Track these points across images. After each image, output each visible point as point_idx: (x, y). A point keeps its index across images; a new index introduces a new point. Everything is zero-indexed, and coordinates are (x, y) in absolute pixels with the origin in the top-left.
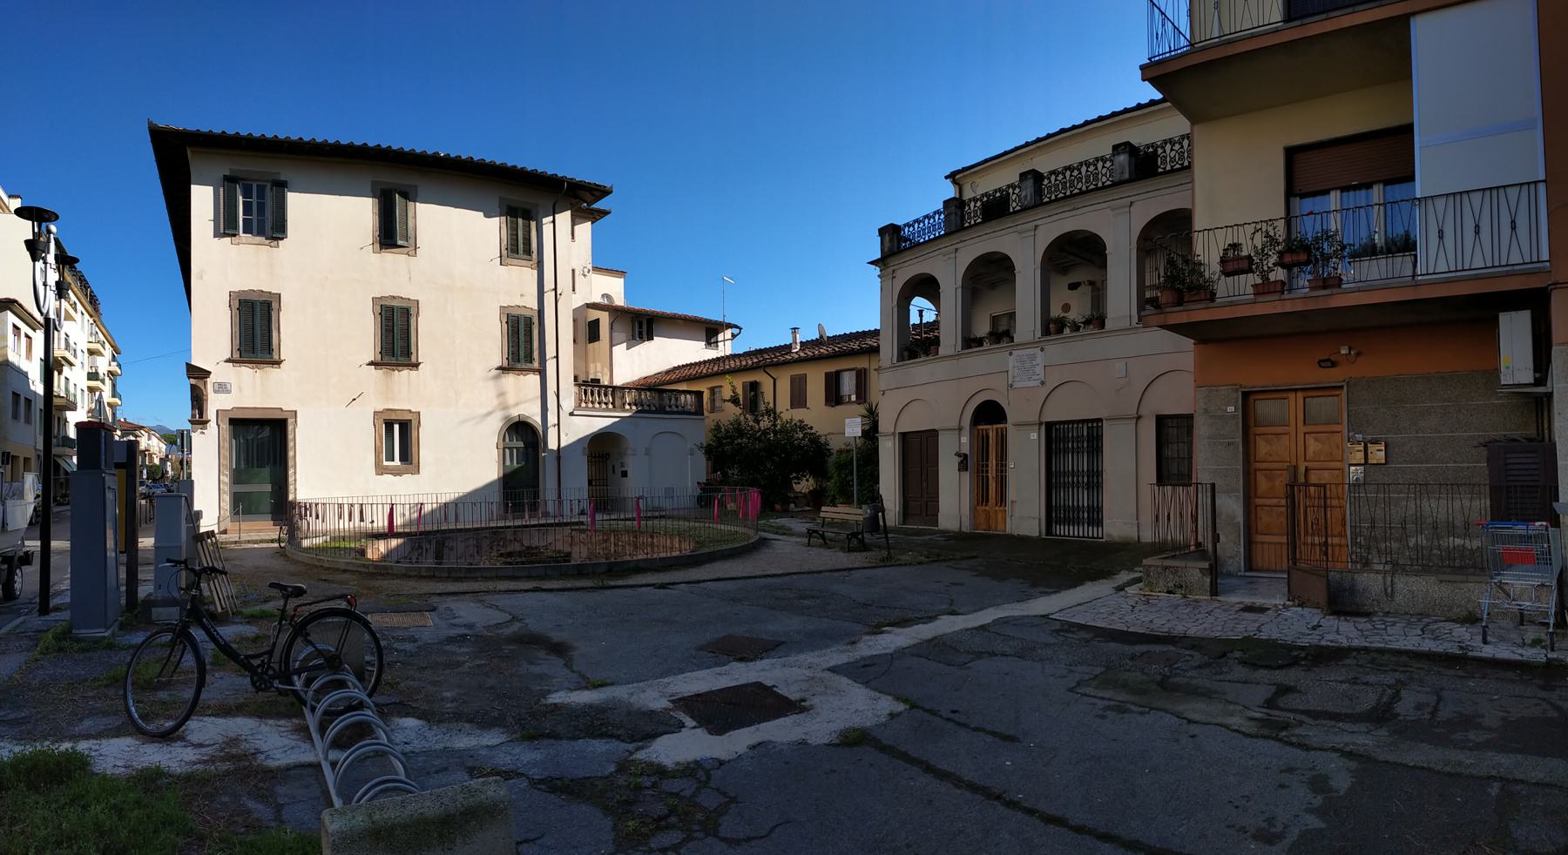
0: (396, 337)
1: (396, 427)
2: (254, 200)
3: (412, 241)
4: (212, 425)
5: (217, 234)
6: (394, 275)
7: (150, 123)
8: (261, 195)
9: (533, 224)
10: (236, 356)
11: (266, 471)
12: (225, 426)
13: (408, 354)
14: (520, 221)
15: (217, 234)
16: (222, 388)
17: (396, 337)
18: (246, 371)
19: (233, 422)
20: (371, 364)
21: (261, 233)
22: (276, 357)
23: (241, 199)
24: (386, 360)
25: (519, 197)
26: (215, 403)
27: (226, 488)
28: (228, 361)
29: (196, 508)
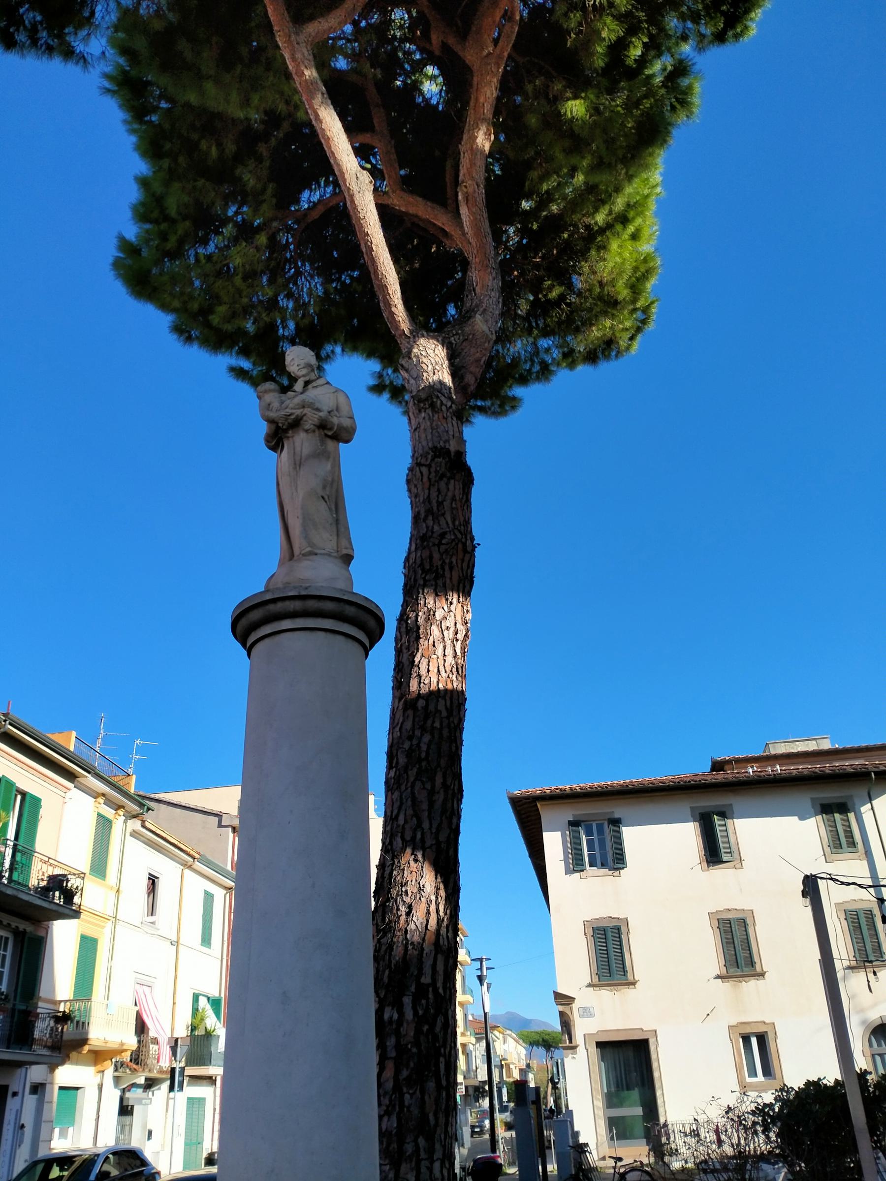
0: (738, 948)
1: (754, 1041)
2: (595, 837)
3: (736, 855)
4: (581, 1050)
5: (568, 872)
6: (725, 889)
7: (508, 793)
8: (601, 831)
9: (851, 816)
10: (596, 980)
11: (635, 1094)
12: (593, 1049)
13: (752, 964)
14: (837, 816)
15: (568, 872)
16: (586, 1012)
17: (738, 948)
18: (605, 994)
19: (599, 1045)
20: (718, 977)
21: (603, 865)
22: (630, 978)
23: (584, 838)
24: (733, 971)
25: (831, 794)
26: (582, 1028)
27: (600, 1113)
28: (589, 985)
29: (576, 1129)
